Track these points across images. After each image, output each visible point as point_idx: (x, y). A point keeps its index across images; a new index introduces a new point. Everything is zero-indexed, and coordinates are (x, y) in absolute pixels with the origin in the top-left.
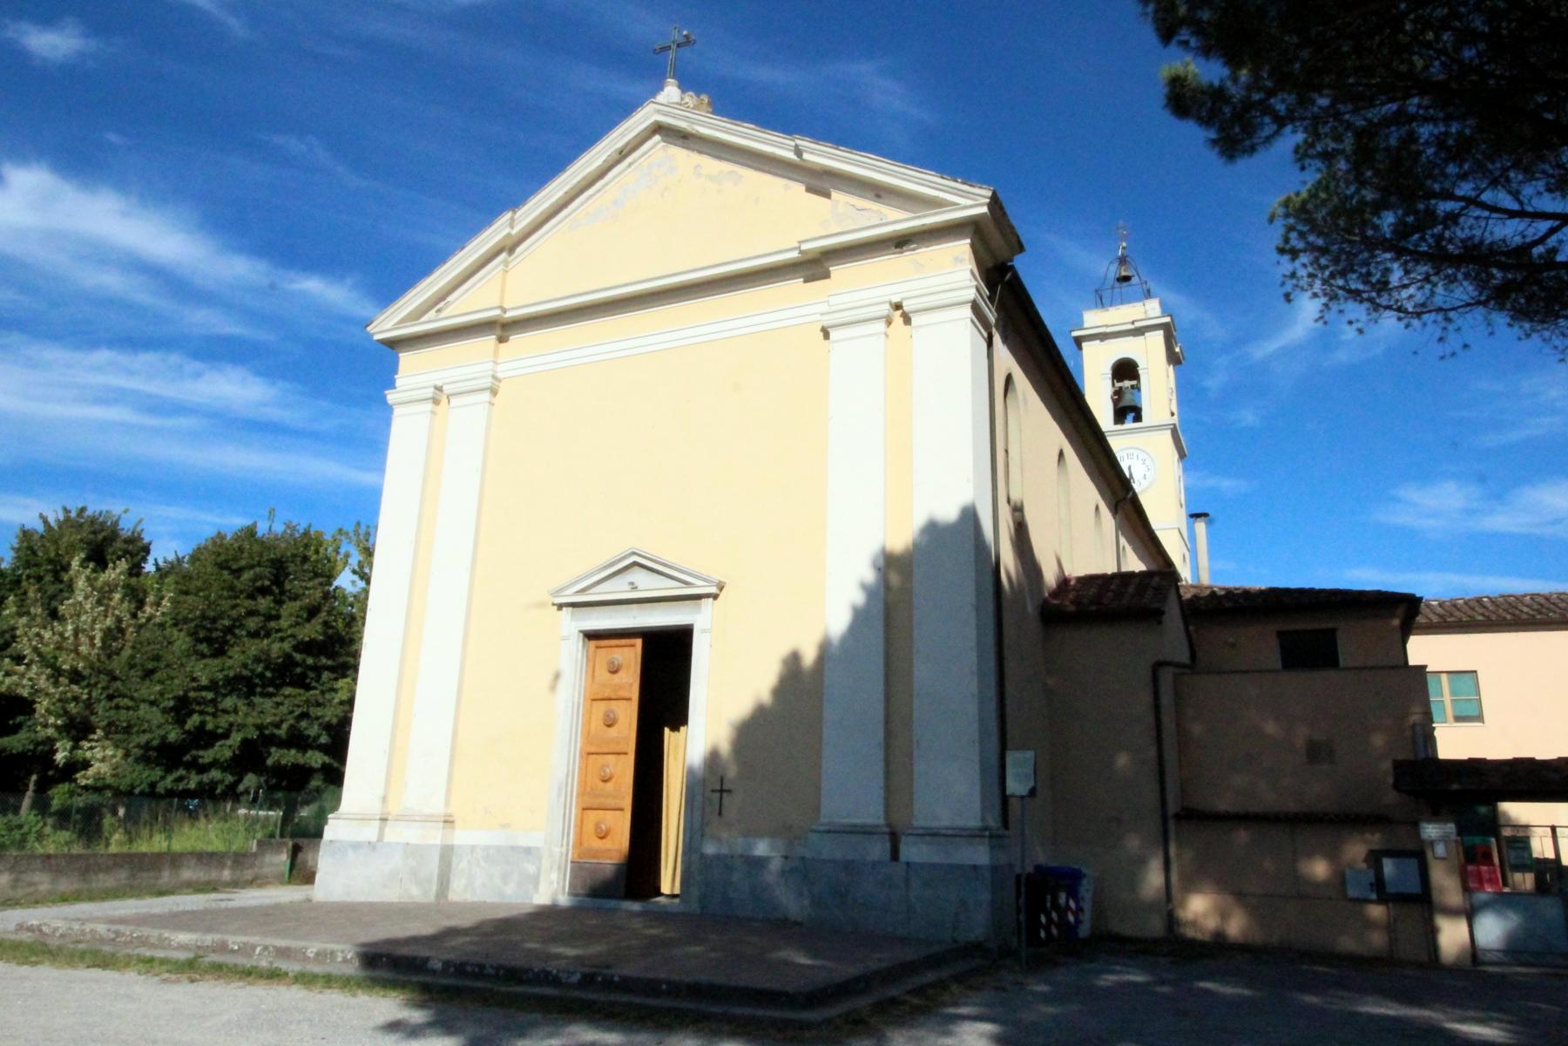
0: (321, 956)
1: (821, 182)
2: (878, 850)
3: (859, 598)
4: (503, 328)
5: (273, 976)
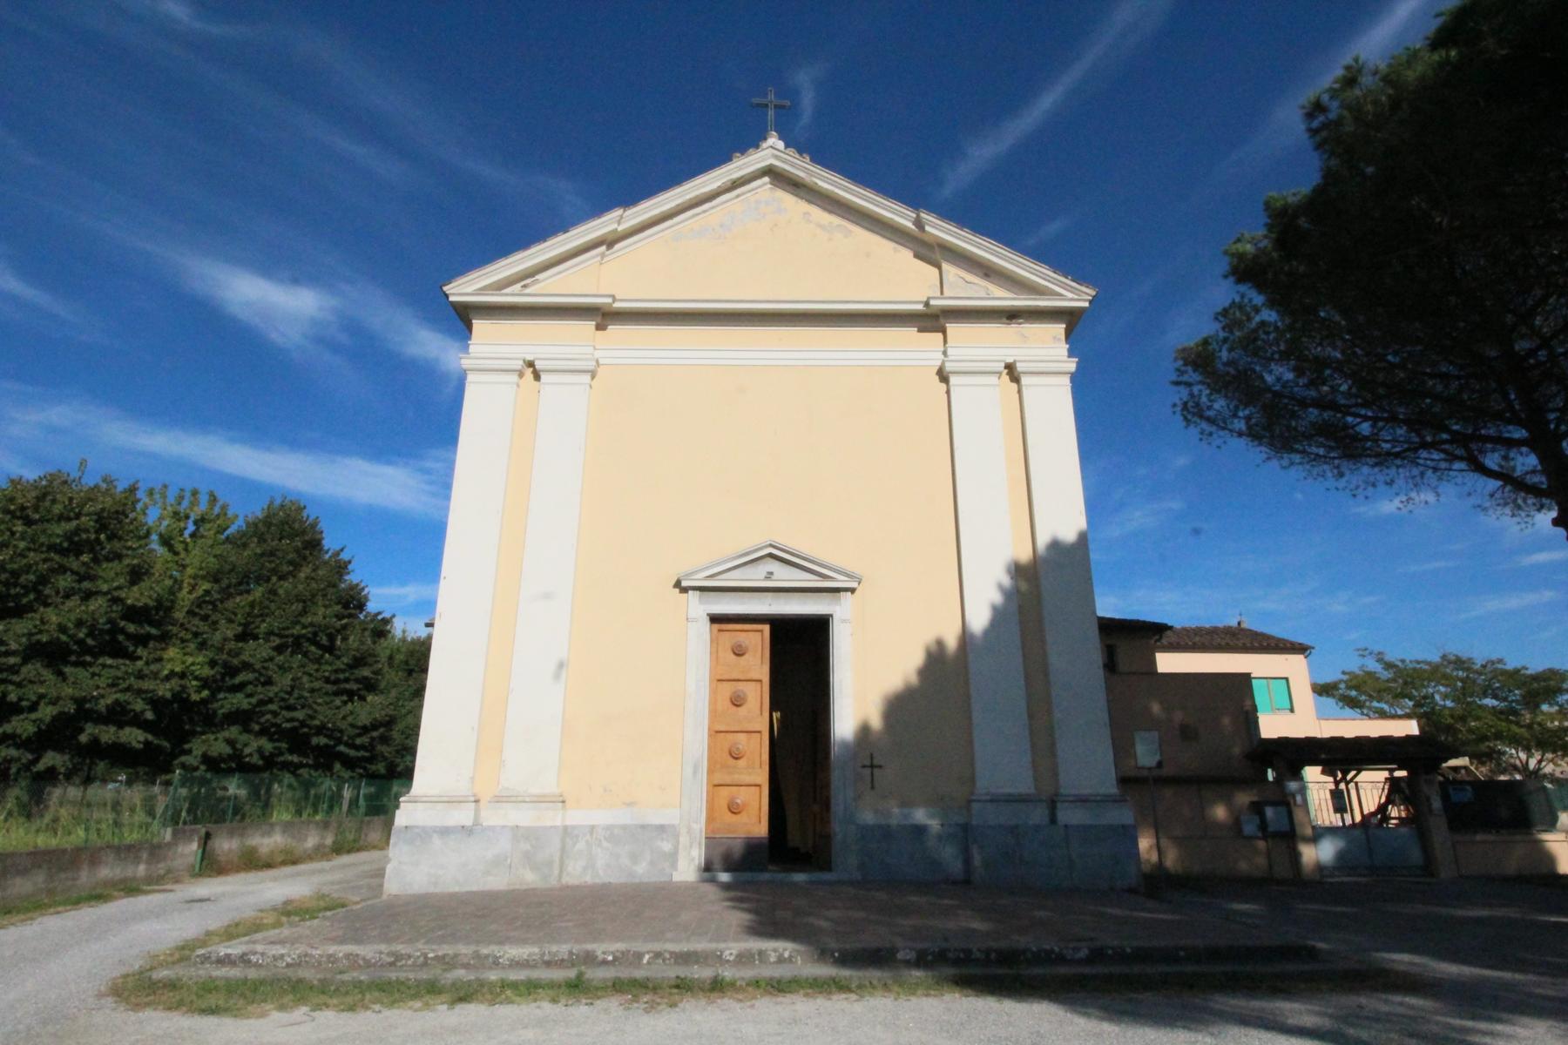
1: (930, 252)
2: (1038, 815)
3: (997, 598)
4: (604, 316)
5: (683, 987)
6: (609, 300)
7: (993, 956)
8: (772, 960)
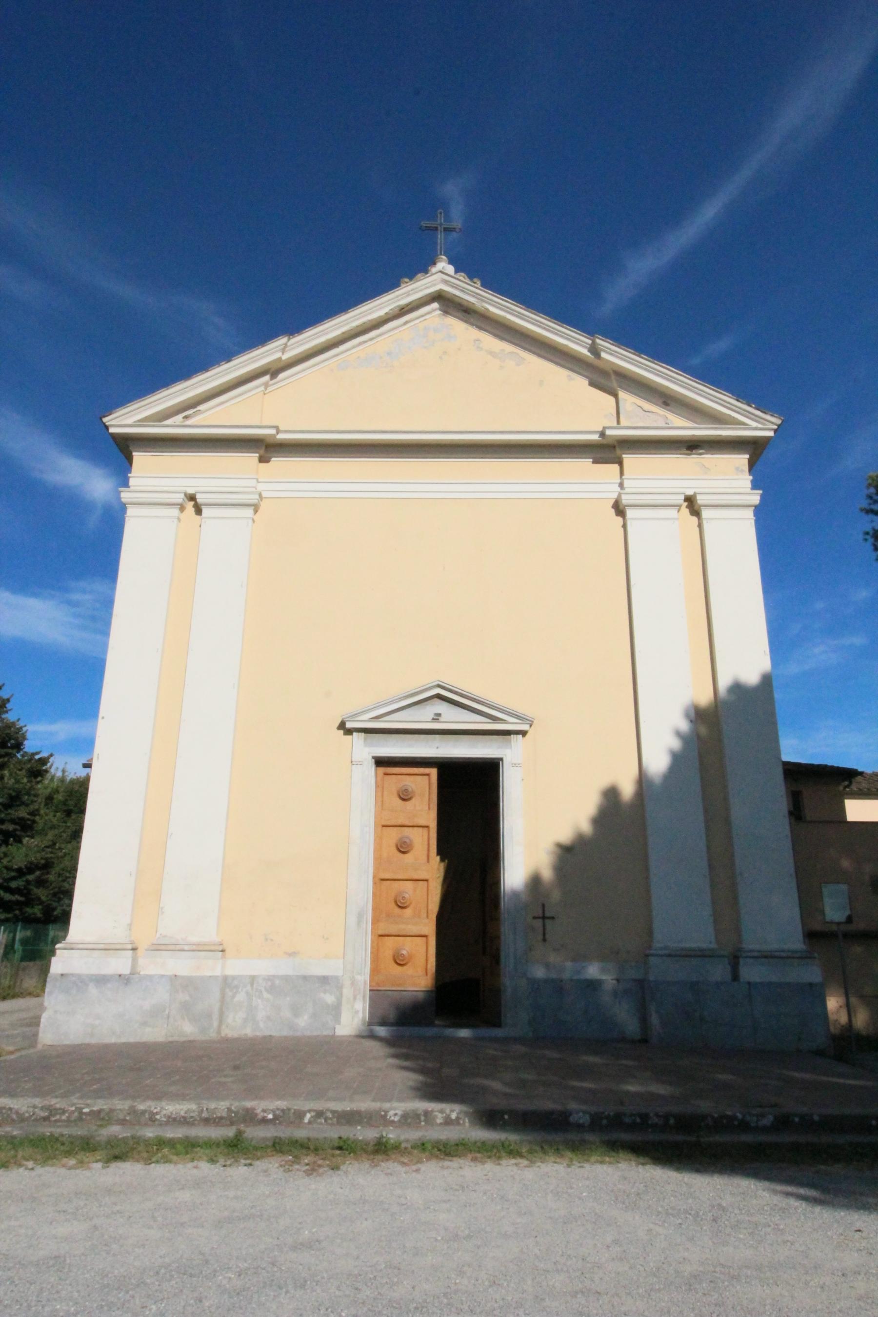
0: (280, 1118)
1: (606, 380)
2: (718, 972)
3: (676, 744)
4: (267, 448)
5: (345, 1148)
6: (273, 431)
7: (672, 1121)
8: (439, 1121)
